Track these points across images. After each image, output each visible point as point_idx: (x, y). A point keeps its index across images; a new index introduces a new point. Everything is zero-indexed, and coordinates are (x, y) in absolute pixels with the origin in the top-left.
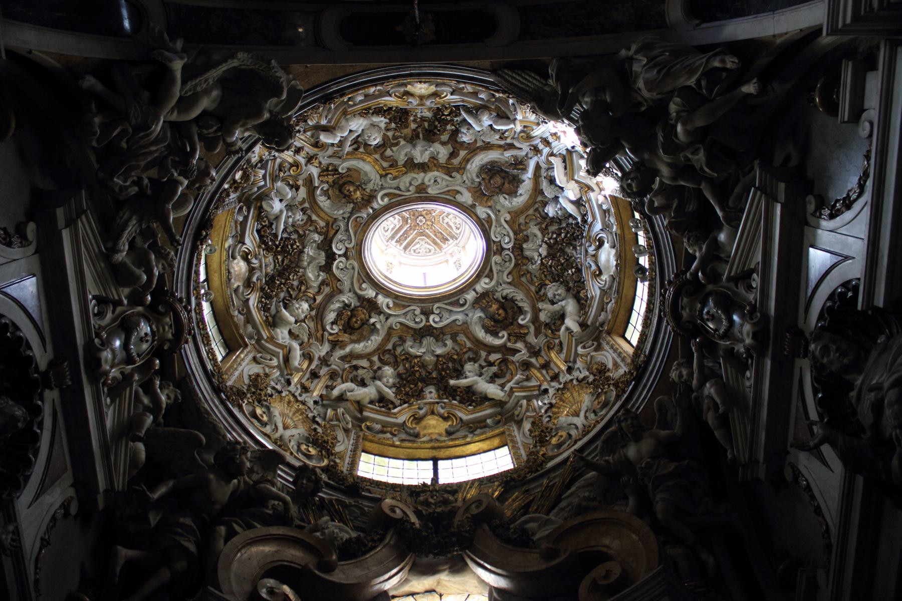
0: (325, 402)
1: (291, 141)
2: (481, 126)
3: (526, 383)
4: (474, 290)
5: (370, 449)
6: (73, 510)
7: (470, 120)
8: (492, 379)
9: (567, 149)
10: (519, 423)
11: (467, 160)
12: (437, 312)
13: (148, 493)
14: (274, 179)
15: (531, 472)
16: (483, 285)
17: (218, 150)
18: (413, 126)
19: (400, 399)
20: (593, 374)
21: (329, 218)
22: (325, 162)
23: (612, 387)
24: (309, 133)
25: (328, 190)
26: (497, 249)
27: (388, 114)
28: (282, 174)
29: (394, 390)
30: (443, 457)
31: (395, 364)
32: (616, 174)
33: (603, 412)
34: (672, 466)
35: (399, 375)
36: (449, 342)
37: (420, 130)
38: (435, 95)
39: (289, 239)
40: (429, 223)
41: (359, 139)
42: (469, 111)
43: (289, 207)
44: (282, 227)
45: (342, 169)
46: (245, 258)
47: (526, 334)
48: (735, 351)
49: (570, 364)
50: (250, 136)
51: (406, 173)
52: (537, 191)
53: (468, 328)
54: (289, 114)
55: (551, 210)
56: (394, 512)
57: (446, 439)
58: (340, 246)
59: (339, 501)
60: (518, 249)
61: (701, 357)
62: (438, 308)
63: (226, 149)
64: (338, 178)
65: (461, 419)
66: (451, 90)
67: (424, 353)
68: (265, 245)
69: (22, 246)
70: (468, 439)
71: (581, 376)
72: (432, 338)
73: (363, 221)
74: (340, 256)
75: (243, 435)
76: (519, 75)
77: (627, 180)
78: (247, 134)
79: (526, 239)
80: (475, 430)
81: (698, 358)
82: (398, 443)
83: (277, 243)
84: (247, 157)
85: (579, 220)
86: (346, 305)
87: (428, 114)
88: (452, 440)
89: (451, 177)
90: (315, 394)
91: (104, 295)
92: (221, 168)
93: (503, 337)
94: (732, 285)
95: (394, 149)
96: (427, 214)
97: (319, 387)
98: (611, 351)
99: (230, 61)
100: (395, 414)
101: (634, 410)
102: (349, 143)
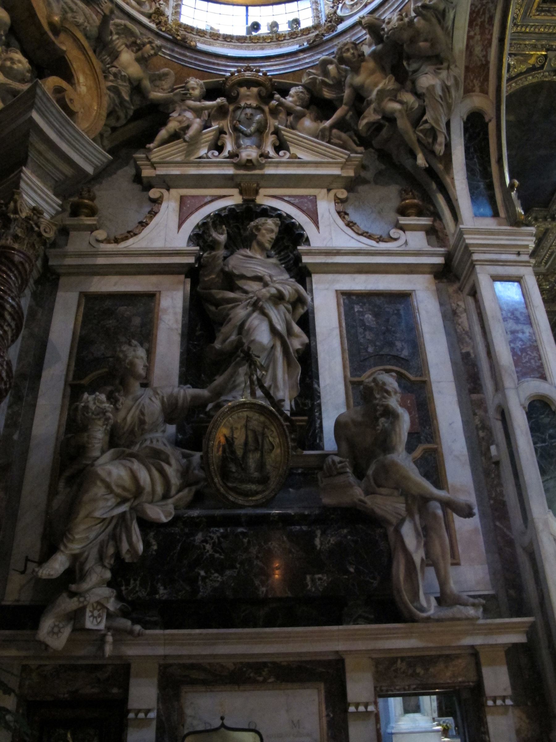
34: (127, 98)
48: (224, 136)
94: (272, 129)
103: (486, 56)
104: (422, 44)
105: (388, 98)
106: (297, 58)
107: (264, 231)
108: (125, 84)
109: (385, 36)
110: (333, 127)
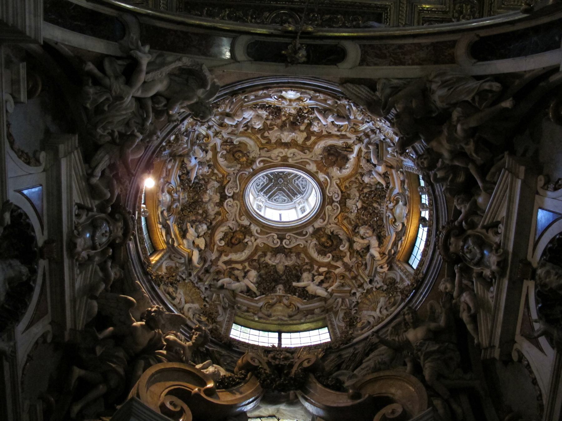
0: (212, 289)
1: (210, 117)
2: (327, 122)
3: (341, 288)
4: (313, 226)
5: (238, 322)
6: (49, 339)
7: (320, 117)
8: (321, 283)
9: (380, 140)
10: (336, 313)
11: (315, 143)
12: (288, 238)
14: (193, 144)
15: (343, 344)
16: (319, 224)
17: (163, 119)
18: (284, 118)
19: (260, 292)
20: (386, 284)
21: (225, 173)
22: (226, 136)
23: (399, 294)
24: (218, 117)
25: (226, 154)
26: (329, 201)
27: (268, 110)
28: (198, 142)
29: (257, 285)
30: (285, 331)
31: (258, 269)
32: (412, 157)
33: (393, 309)
35: (260, 276)
36: (294, 258)
37: (287, 121)
38: (299, 99)
39: (197, 183)
40: (286, 183)
41: (249, 124)
42: (319, 111)
43: (201, 163)
44: (195, 175)
45: (236, 142)
46: (169, 193)
47: (344, 257)
49: (371, 278)
50: (184, 112)
51: (276, 148)
52: (358, 165)
53: (306, 250)
54: (210, 100)
55: (366, 179)
56: (254, 361)
57: (288, 319)
58: (230, 191)
59: (219, 353)
60: (343, 203)
61: (461, 276)
62: (289, 235)
63: (168, 119)
64: (232, 147)
65: (298, 308)
66: (310, 97)
67: (278, 264)
68: (183, 186)
69: (36, 166)
70: (302, 321)
71: (378, 286)
72: (283, 255)
73: (246, 177)
74: (229, 197)
76: (359, 89)
77: (421, 159)
78: (182, 110)
79: (349, 197)
80: (307, 315)
81: (459, 277)
82: (257, 319)
83: (191, 185)
84: (179, 127)
85: (384, 186)
86: (230, 228)
87: (293, 112)
88: (292, 320)
89: (305, 153)
90: (206, 283)
91: (83, 203)
92: (163, 131)
93: (329, 257)
94: (484, 231)
95: (270, 132)
96: (284, 177)
97: (209, 279)
98: (399, 271)
99: (177, 62)
100: (256, 300)
101: (414, 308)
102: (242, 126)
103: (427, 46)
104: (414, 105)
105: (455, 134)
106: (438, 197)
107: (548, 280)
108: (426, 345)
109: (406, 136)
110: (483, 180)
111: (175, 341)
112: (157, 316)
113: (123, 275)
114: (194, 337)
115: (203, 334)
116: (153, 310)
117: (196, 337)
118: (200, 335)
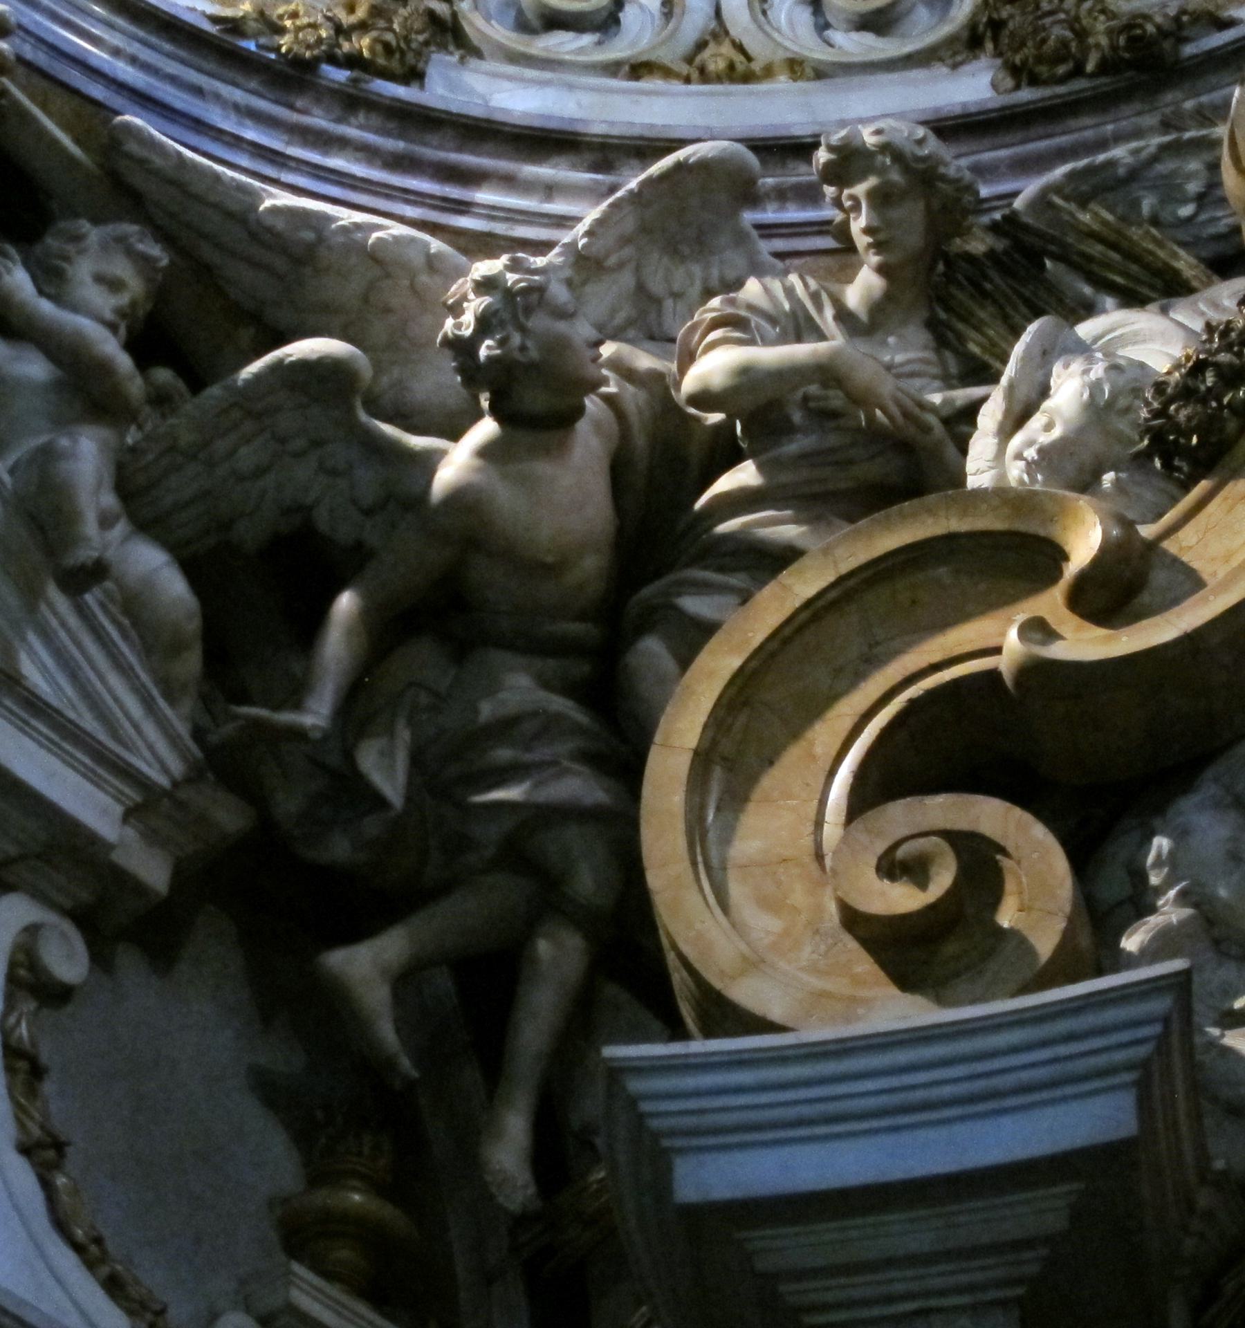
13: (286, 717)
75: (530, 170)
111: (746, 375)
112: (516, 339)
113: (155, 250)
114: (858, 224)
115: (896, 176)
116: (468, 319)
117: (868, 231)
118: (881, 199)
